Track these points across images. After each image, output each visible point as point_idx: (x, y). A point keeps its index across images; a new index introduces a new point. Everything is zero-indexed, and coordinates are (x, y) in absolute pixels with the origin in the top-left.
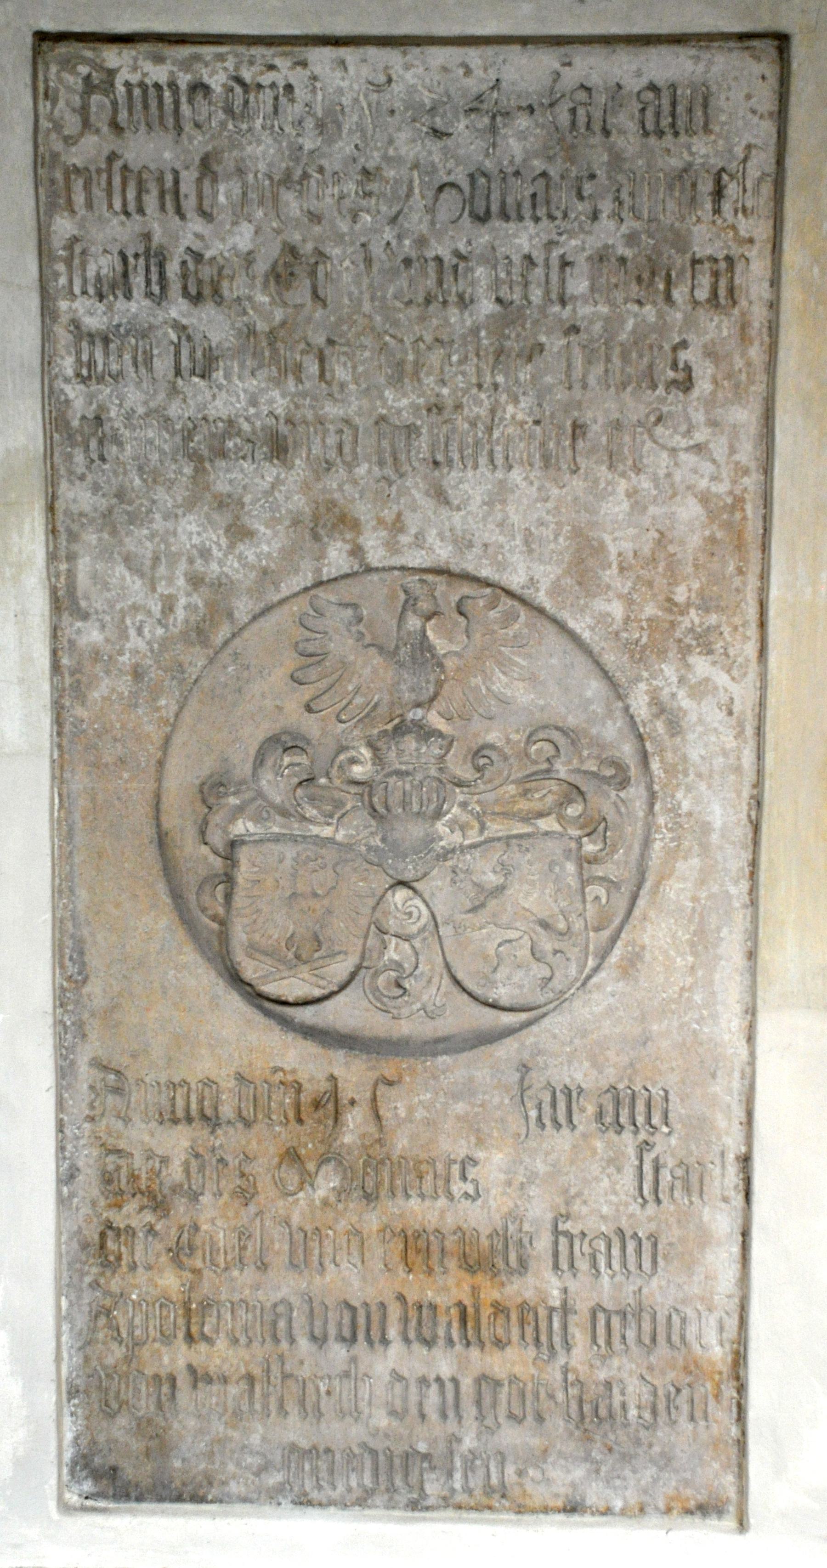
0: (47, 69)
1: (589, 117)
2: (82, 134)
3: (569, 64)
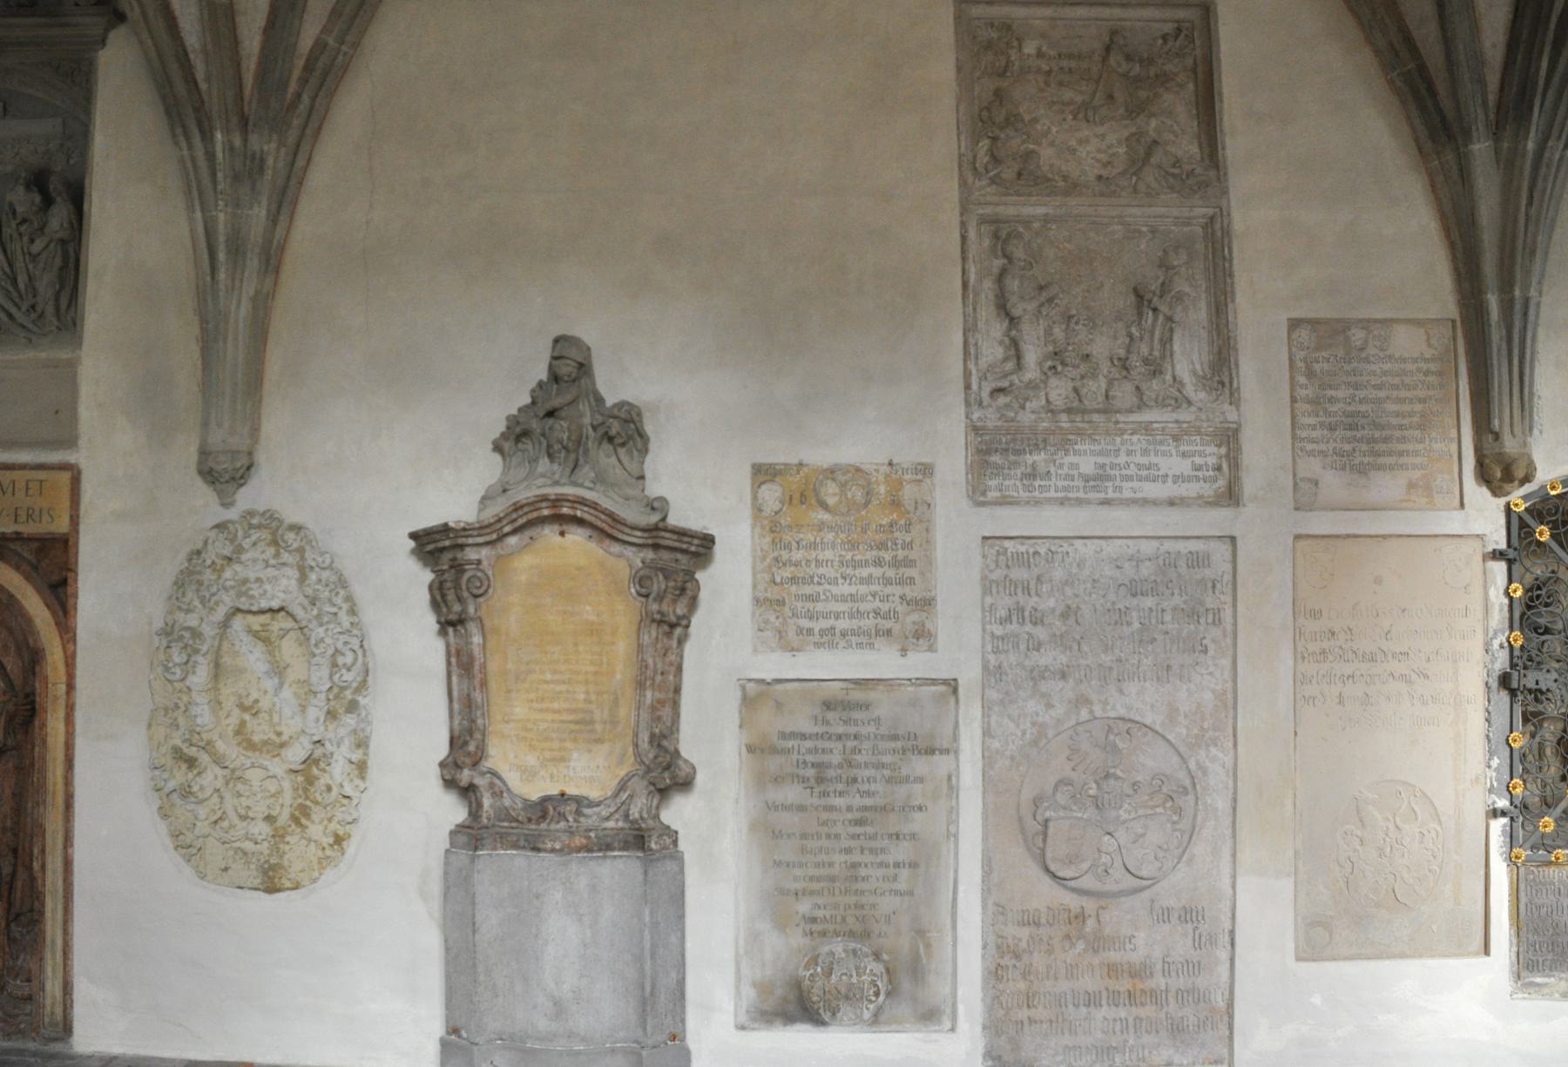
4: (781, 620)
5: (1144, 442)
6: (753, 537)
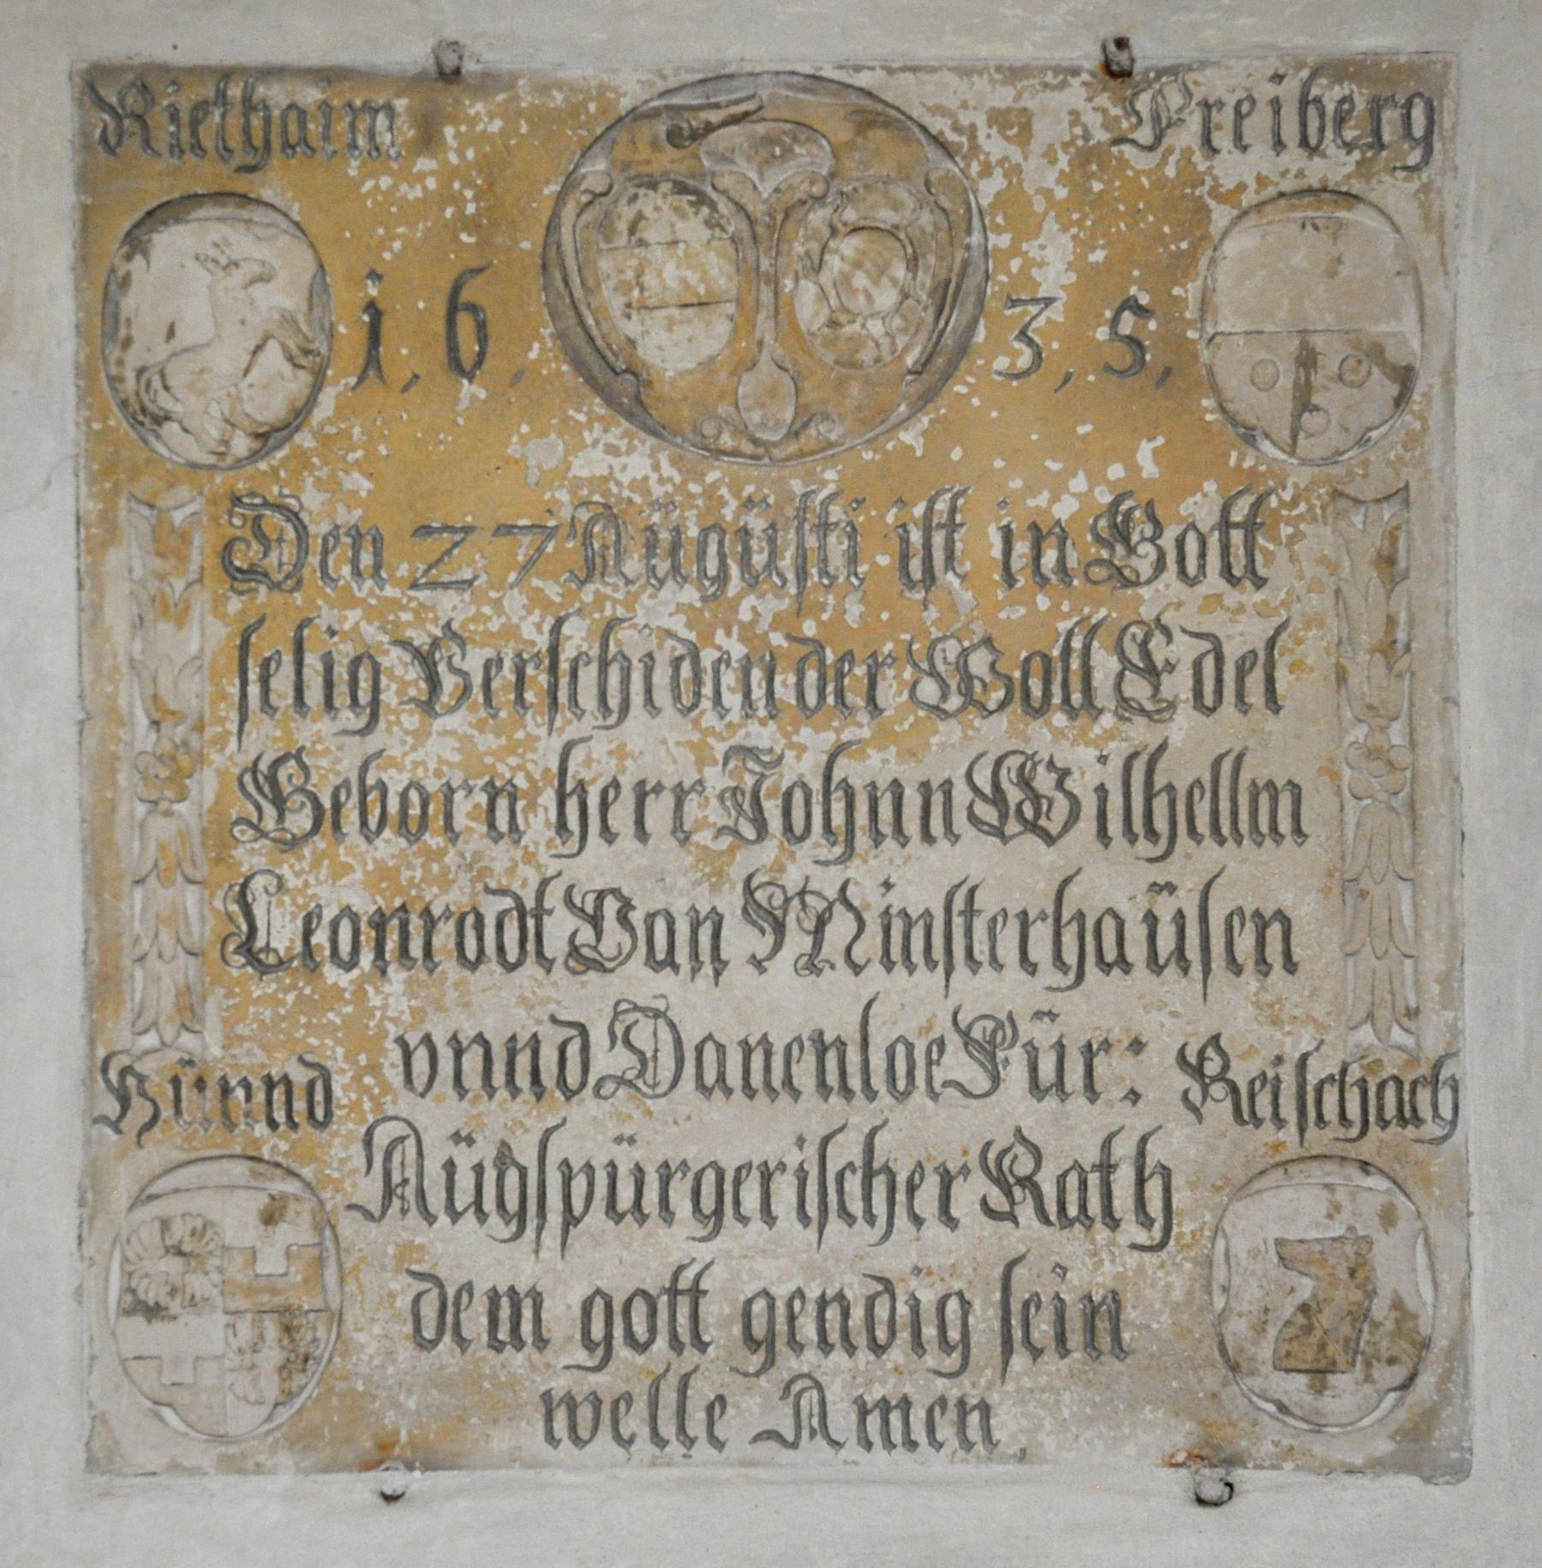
4: (296, 1231)
6: (91, 619)
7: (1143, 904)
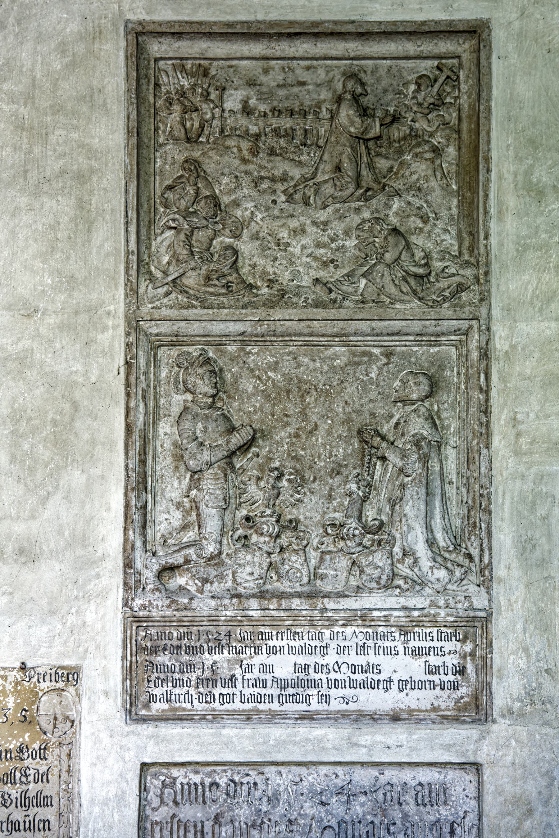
0: (146, 778)
1: (392, 796)
2: (160, 807)
3: (383, 774)
5: (361, 636)
7: (23, 819)
